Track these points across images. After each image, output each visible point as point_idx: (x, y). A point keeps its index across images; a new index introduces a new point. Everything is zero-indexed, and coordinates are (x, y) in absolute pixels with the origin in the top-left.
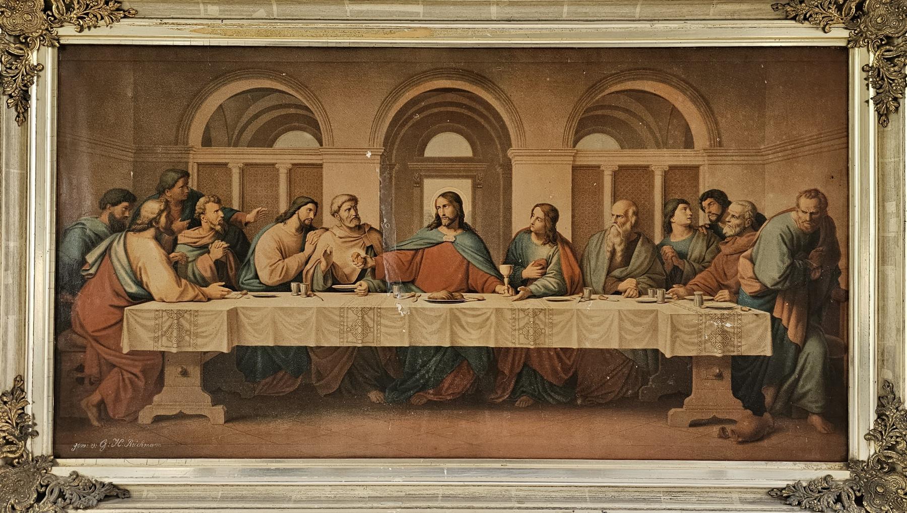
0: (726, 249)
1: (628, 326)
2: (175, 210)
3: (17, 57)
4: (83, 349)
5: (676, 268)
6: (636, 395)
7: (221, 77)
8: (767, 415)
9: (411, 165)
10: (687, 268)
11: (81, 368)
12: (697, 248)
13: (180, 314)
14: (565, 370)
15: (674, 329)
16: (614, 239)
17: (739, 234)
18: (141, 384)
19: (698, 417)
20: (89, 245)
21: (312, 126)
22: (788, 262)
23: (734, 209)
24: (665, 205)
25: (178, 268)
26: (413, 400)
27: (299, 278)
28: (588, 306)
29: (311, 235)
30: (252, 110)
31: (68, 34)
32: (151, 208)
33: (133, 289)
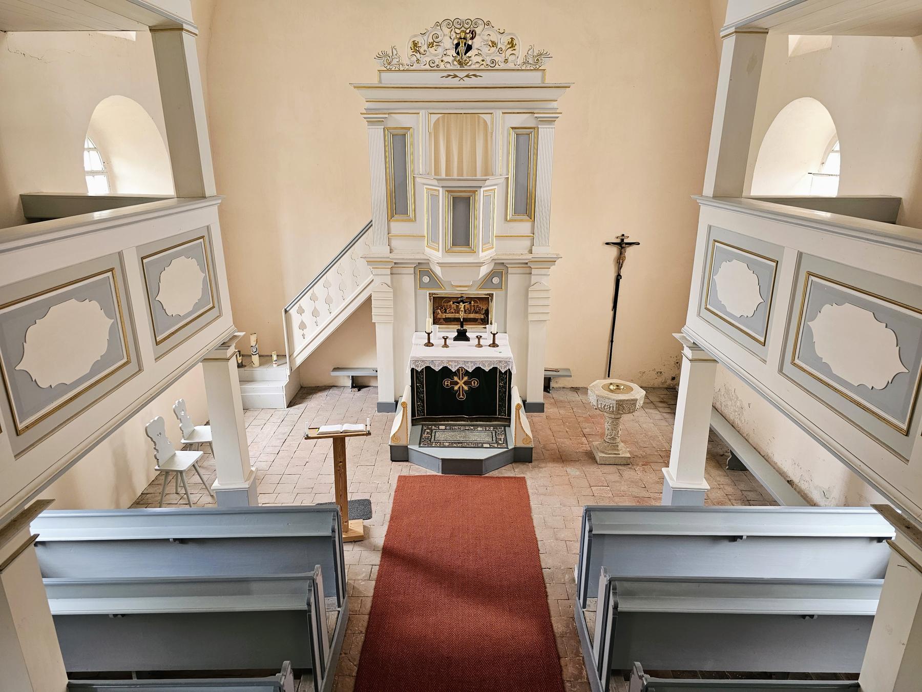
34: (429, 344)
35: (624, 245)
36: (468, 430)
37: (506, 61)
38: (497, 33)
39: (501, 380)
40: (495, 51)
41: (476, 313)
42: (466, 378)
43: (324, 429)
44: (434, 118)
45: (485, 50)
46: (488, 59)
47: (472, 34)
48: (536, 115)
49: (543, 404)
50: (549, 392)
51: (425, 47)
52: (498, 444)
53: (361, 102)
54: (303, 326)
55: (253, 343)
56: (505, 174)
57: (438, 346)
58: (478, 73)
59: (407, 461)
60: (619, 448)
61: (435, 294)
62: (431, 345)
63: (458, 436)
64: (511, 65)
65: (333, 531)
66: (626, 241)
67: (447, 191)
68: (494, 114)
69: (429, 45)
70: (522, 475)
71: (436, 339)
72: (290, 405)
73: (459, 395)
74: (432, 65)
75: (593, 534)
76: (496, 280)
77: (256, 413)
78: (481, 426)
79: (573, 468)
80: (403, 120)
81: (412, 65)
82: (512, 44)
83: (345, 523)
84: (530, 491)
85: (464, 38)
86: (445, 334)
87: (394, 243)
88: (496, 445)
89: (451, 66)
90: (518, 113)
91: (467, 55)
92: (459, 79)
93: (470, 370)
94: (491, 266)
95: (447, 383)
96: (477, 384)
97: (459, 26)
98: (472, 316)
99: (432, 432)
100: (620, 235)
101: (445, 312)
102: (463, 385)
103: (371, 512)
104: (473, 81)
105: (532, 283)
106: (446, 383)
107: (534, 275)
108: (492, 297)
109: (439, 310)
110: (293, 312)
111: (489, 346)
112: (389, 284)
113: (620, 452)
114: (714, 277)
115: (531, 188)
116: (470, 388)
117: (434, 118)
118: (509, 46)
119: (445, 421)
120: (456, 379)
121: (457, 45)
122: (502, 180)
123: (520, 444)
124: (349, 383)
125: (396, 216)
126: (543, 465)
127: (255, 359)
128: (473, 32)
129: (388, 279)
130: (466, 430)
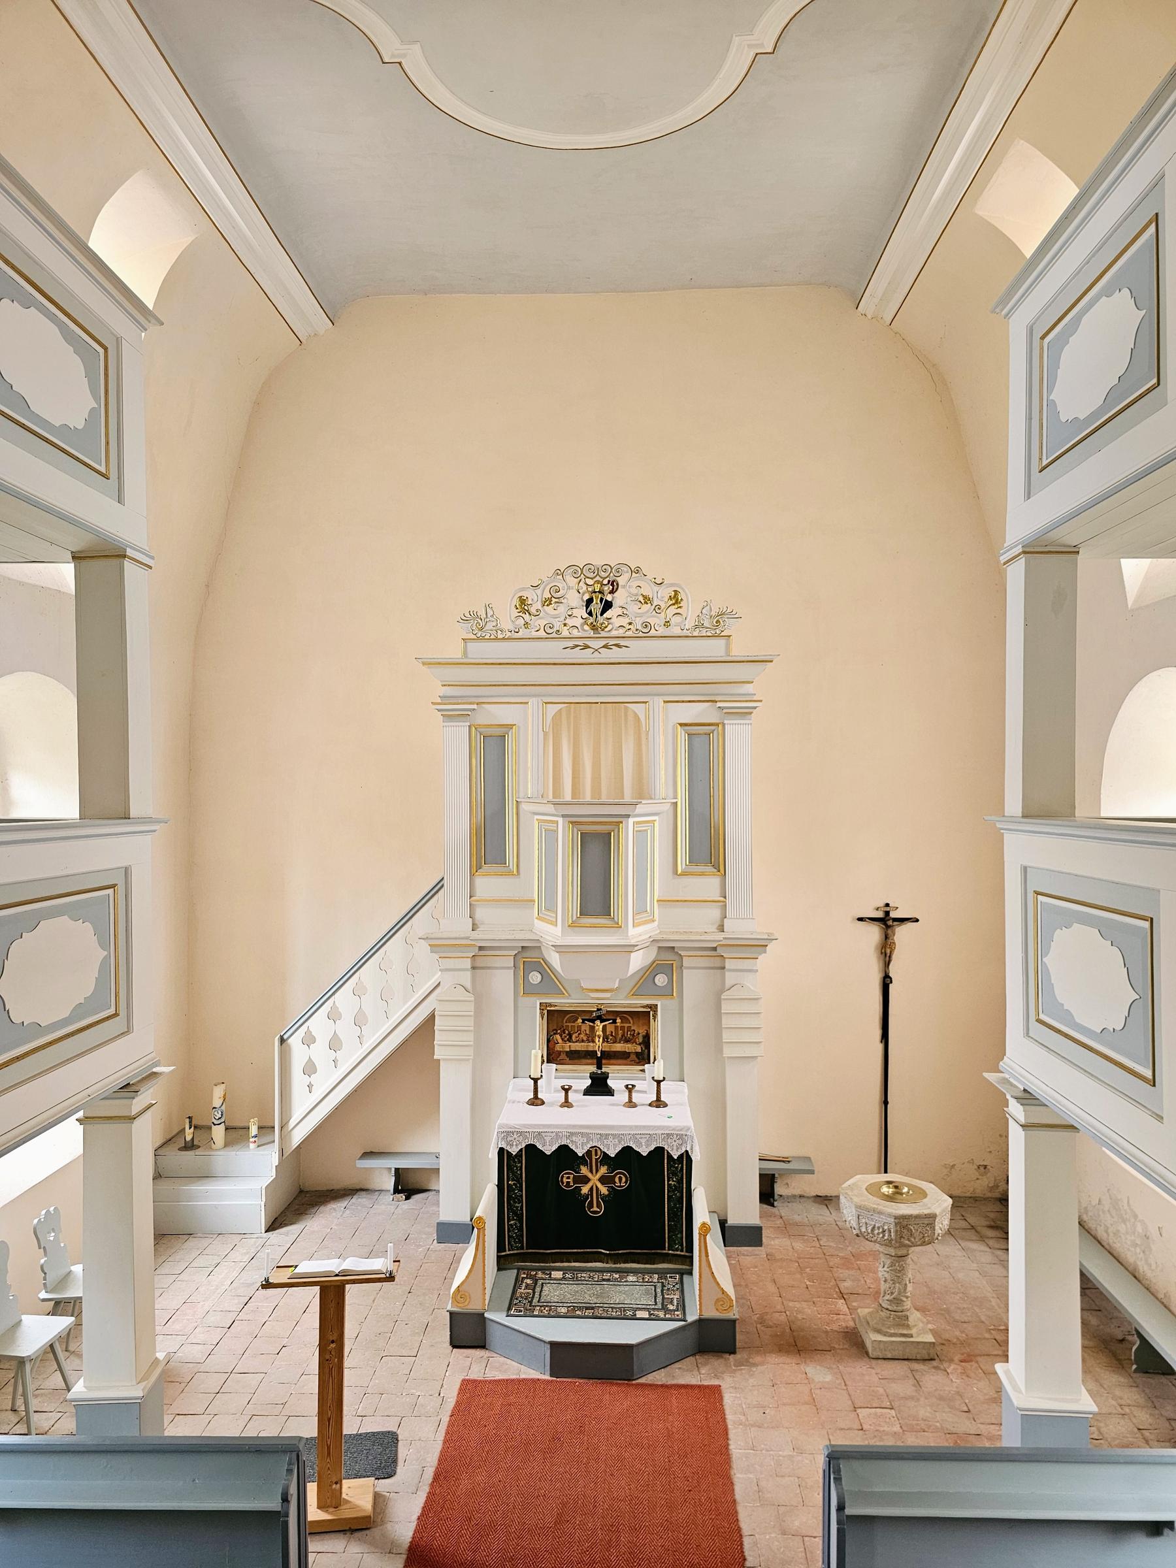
12: (631, 1037)
16: (620, 1036)
25: (562, 1039)
31: (548, 1008)
32: (559, 1031)
34: (536, 1101)
35: (890, 923)
36: (608, 1280)
37: (667, 624)
38: (652, 585)
39: (673, 1173)
40: (650, 609)
41: (627, 1041)
42: (603, 1170)
43: (306, 1267)
44: (552, 710)
45: (633, 608)
46: (638, 623)
47: (612, 584)
48: (719, 704)
49: (761, 1228)
50: (772, 1205)
51: (538, 605)
52: (667, 1311)
53: (434, 686)
54: (310, 1069)
55: (217, 1102)
56: (672, 796)
57: (552, 1104)
58: (622, 643)
59: (483, 1346)
60: (911, 1321)
61: (550, 1005)
62: (540, 1102)
63: (585, 1293)
64: (676, 631)
65: (285, 1499)
66: (893, 915)
67: (572, 823)
68: (651, 703)
69: (545, 602)
70: (715, 1382)
71: (550, 1091)
72: (272, 1227)
73: (591, 1204)
74: (550, 631)
75: (847, 1516)
76: (661, 980)
77: (205, 1242)
78: (635, 1272)
79: (818, 1367)
80: (500, 714)
81: (517, 630)
82: (676, 599)
83: (334, 1486)
84: (730, 1417)
85: (600, 592)
86: (566, 1082)
87: (480, 913)
88: (661, 1315)
89: (579, 632)
90: (689, 701)
91: (605, 615)
92: (593, 650)
94: (652, 954)
95: (567, 1178)
96: (626, 1182)
97: (592, 575)
98: (619, 1047)
99: (536, 1284)
100: (882, 904)
101: (570, 1040)
102: (599, 1185)
103: (395, 1461)
104: (615, 654)
105: (727, 986)
106: (565, 1180)
107: (730, 970)
108: (655, 1012)
109: (558, 1037)
110: (295, 1042)
111: (650, 1105)
112: (469, 985)
113: (914, 1331)
114: (1044, 959)
115: (716, 820)
116: (612, 1190)
117: (552, 710)
118: (671, 602)
119: (563, 1262)
120: (584, 1170)
121: (589, 602)
122: (667, 807)
123: (711, 1313)
124: (389, 1183)
125: (485, 867)
126: (758, 1359)
127: (218, 1133)
128: (613, 582)
129: (466, 978)
130: (604, 1280)
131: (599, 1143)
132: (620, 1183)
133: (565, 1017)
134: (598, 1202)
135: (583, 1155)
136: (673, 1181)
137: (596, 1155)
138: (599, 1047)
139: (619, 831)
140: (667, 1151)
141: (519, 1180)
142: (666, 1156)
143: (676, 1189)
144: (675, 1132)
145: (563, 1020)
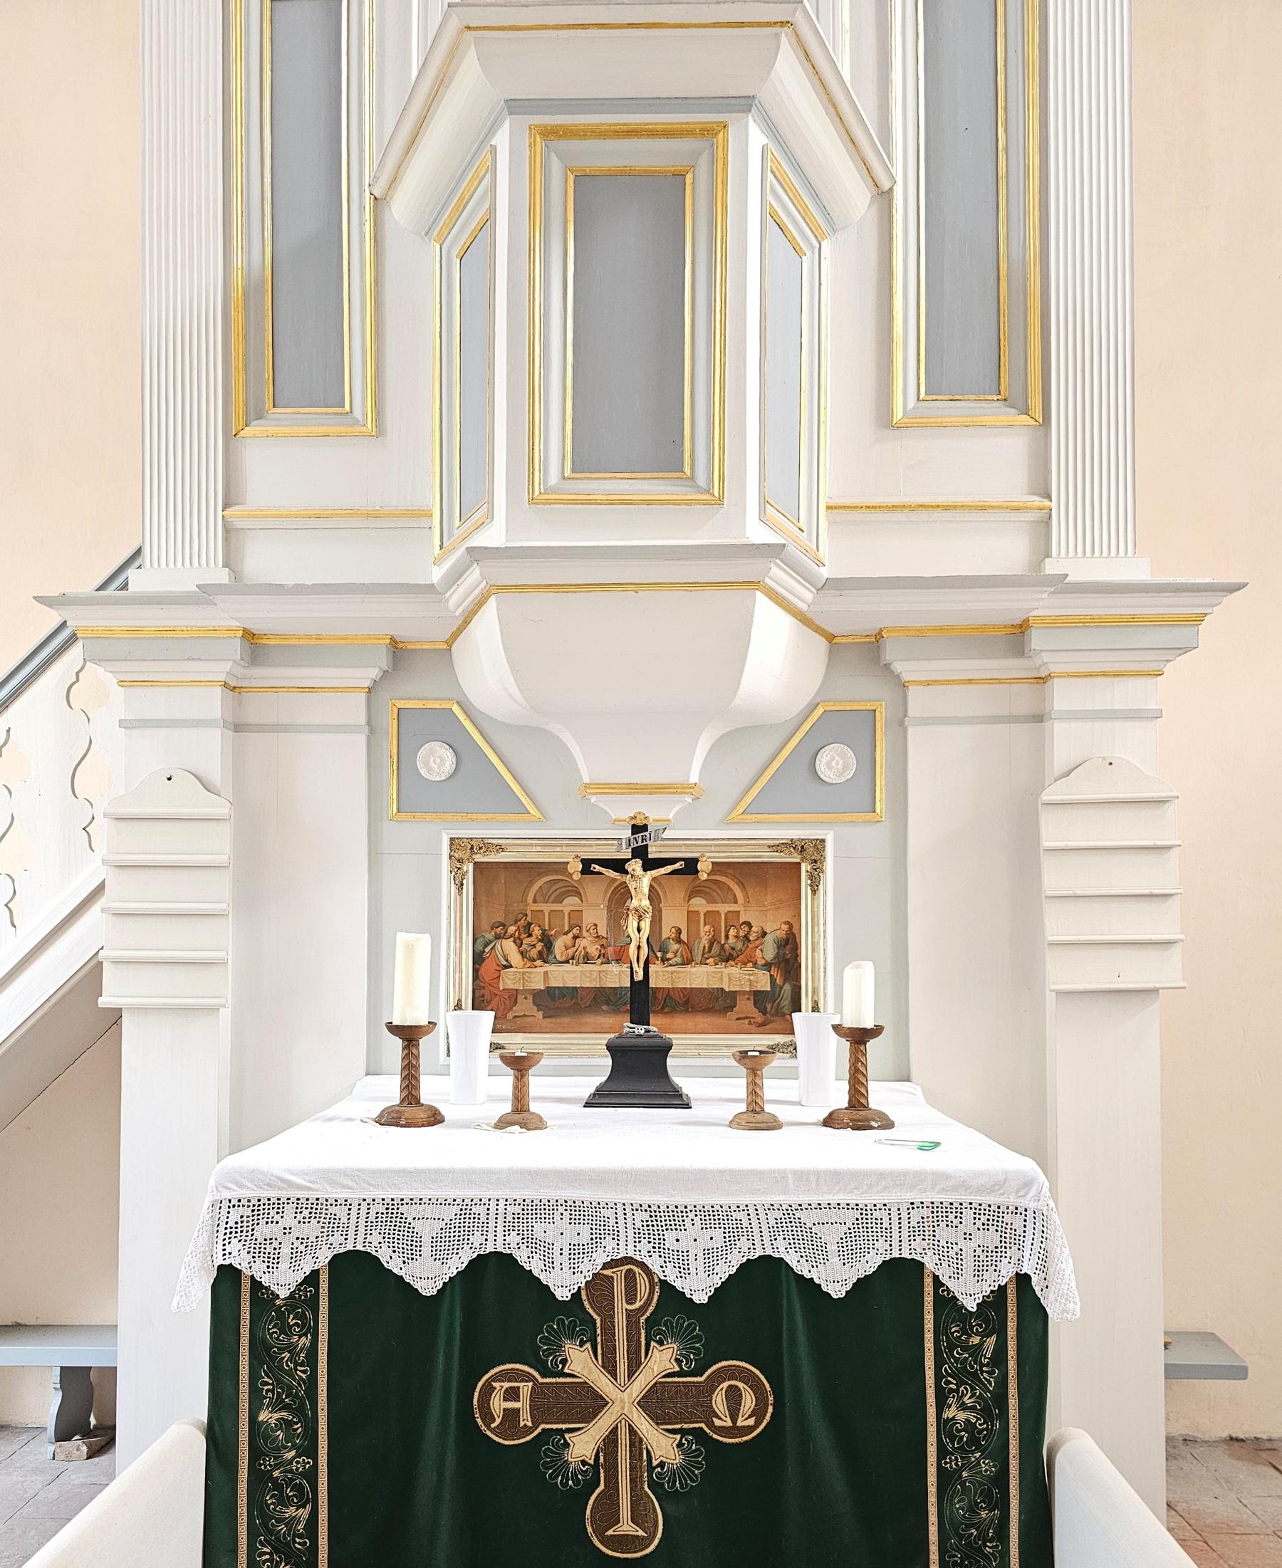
0: (751, 946)
1: (710, 978)
2: (522, 930)
3: (459, 869)
4: (484, 988)
5: (730, 954)
6: (713, 1007)
7: (541, 875)
8: (768, 1015)
9: (619, 910)
10: (735, 954)
11: (483, 996)
12: (739, 946)
13: (524, 973)
14: (685, 996)
15: (730, 979)
16: (705, 942)
17: (756, 940)
18: (508, 1003)
19: (739, 1016)
20: (486, 945)
21: (579, 894)
22: (776, 951)
23: (754, 929)
24: (726, 927)
26: (621, 1009)
27: (573, 958)
28: (694, 970)
29: (578, 940)
30: (553, 889)
31: (479, 858)
32: (512, 929)
33: (505, 963)
41: (727, 957)
61: (484, 846)
62: (421, 1115)
93: (699, 1288)
96: (758, 1413)
98: (700, 976)
101: (546, 954)
102: (644, 1426)
106: (498, 1405)
109: (509, 946)
131: (645, 1246)
132: (734, 1420)
133: (531, 883)
134: (638, 1501)
135: (576, 1296)
136: (963, 1407)
137: (631, 1298)
138: (639, 947)
139: (713, 161)
140: (937, 1281)
141: (302, 1407)
142: (929, 1300)
143: (974, 1441)
144: (966, 1199)
145: (525, 893)
